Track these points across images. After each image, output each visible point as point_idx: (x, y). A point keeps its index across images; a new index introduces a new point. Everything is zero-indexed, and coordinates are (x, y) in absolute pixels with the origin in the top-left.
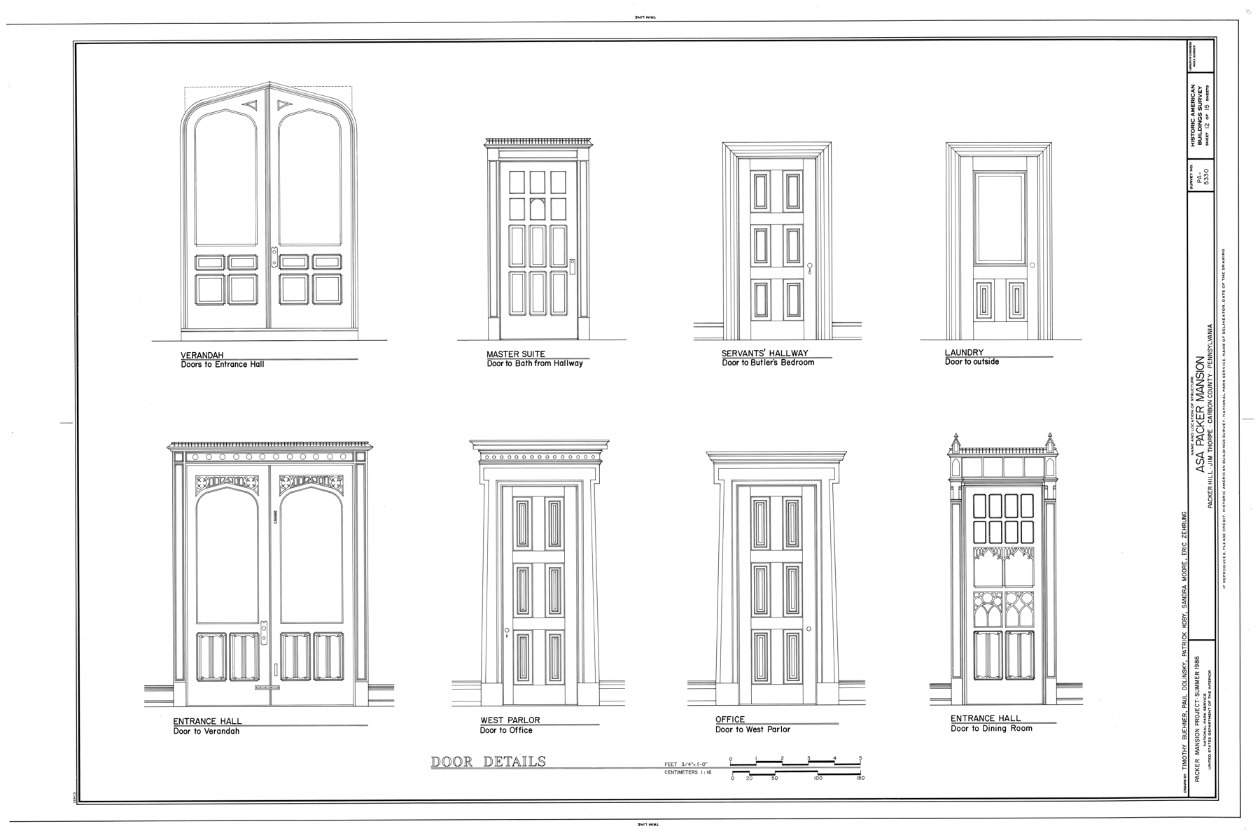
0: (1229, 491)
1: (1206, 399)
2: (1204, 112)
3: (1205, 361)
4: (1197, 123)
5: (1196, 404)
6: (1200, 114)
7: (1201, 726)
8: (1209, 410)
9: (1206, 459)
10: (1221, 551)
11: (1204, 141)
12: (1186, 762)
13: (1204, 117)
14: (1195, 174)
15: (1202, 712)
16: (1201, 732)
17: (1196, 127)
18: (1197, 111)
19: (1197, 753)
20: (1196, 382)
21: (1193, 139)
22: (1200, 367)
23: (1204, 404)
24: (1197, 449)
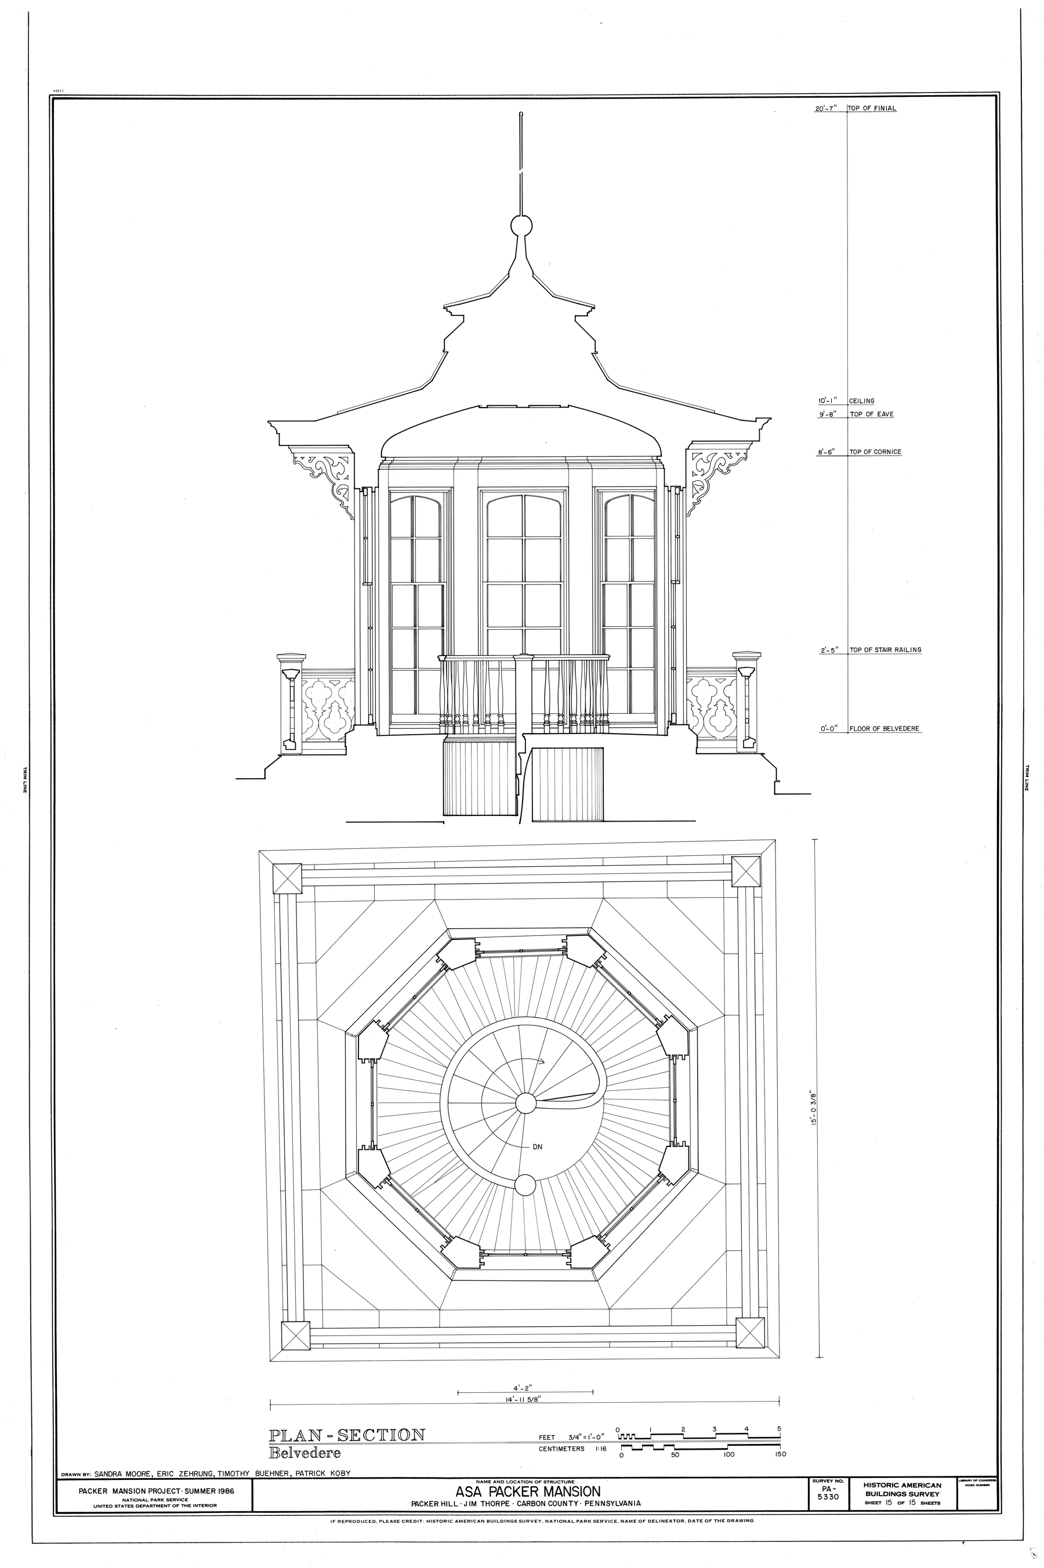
0: (424, 1529)
1: (547, 1499)
2: (907, 1499)
3: (596, 1498)
4: (894, 1490)
5: (541, 1486)
6: (904, 1494)
7: (148, 1496)
8: (533, 1503)
9: (473, 1499)
10: (377, 1518)
11: (870, 1499)
12: (101, 1476)
13: (901, 1499)
14: (833, 1484)
15: (165, 1496)
16: (141, 1496)
17: (889, 1489)
18: (908, 1490)
19: (115, 1491)
20: (568, 1486)
21: (874, 1485)
22: (587, 1491)
23: (541, 1496)
24: (484, 1488)
